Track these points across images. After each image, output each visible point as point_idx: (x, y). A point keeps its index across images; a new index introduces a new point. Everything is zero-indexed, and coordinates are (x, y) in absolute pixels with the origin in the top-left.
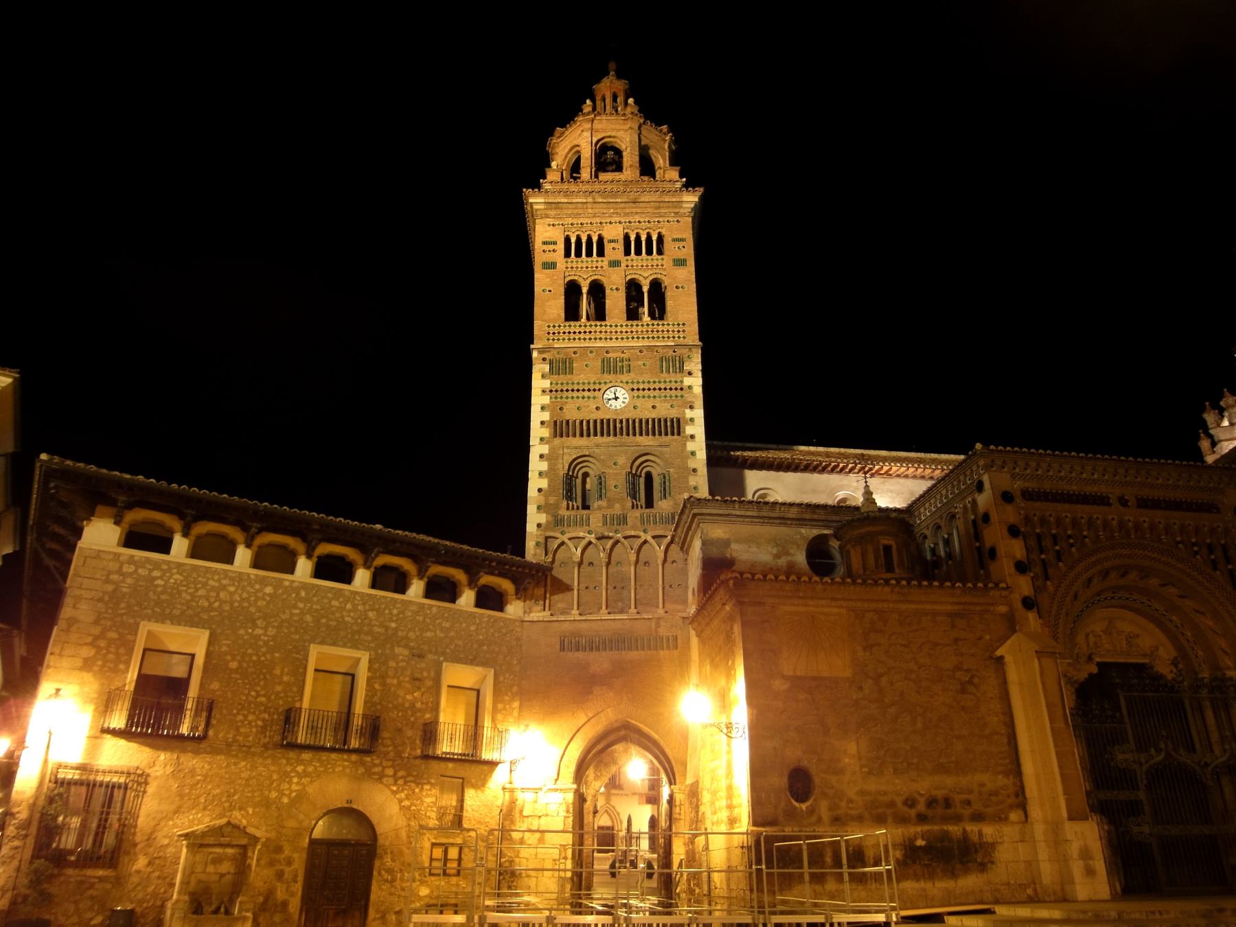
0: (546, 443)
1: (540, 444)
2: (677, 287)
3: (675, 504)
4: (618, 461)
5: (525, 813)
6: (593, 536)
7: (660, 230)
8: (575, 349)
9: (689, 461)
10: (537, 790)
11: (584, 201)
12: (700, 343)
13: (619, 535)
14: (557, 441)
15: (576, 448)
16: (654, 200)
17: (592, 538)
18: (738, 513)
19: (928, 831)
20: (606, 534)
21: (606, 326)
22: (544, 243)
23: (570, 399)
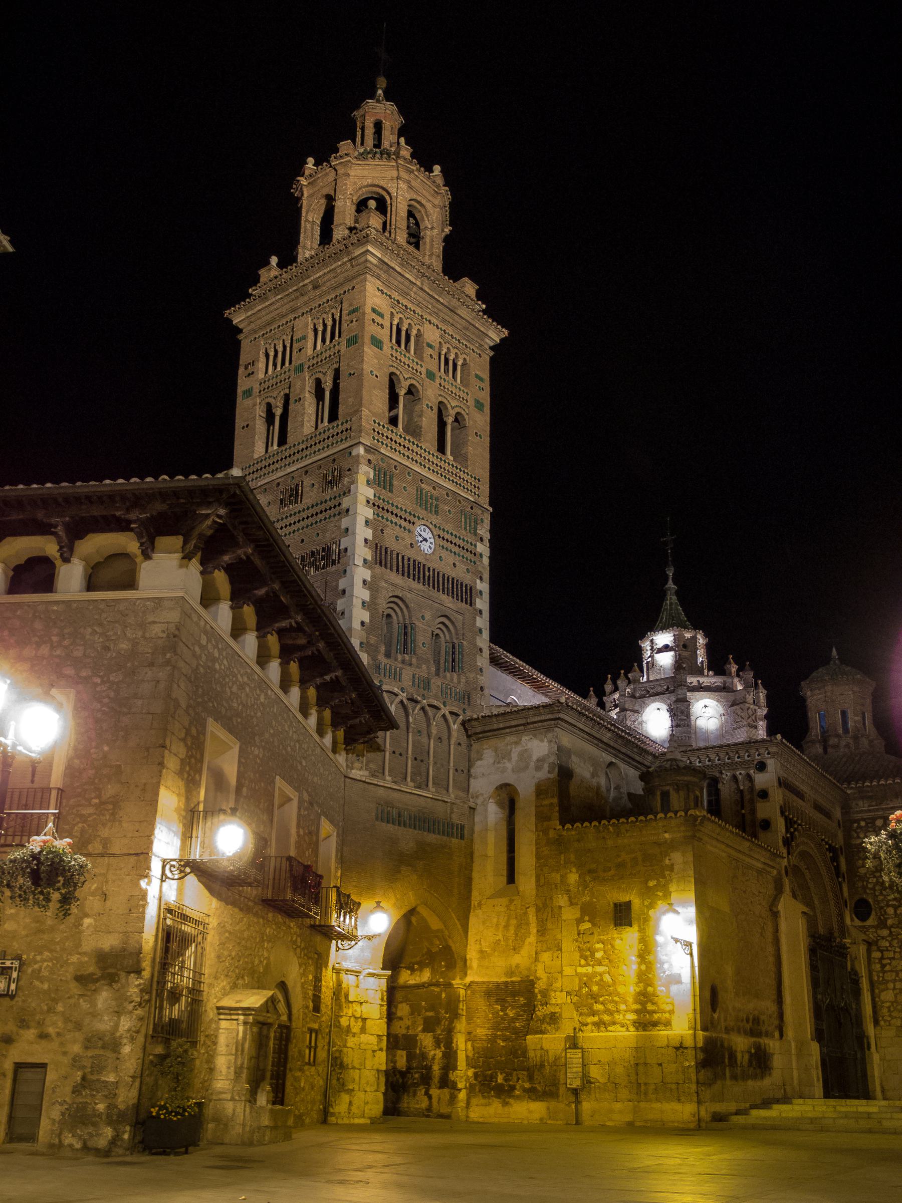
0: (370, 568)
1: (363, 566)
2: (476, 433)
3: (467, 682)
4: (425, 615)
5: (350, 999)
6: (405, 695)
7: (465, 356)
8: (396, 464)
9: (478, 637)
10: (357, 973)
11: (414, 281)
12: (491, 509)
13: (425, 701)
14: (379, 570)
15: (392, 584)
16: (468, 318)
17: (403, 696)
18: (581, 726)
19: (755, 1042)
20: (415, 696)
21: (421, 448)
22: (374, 310)
23: (389, 523)
